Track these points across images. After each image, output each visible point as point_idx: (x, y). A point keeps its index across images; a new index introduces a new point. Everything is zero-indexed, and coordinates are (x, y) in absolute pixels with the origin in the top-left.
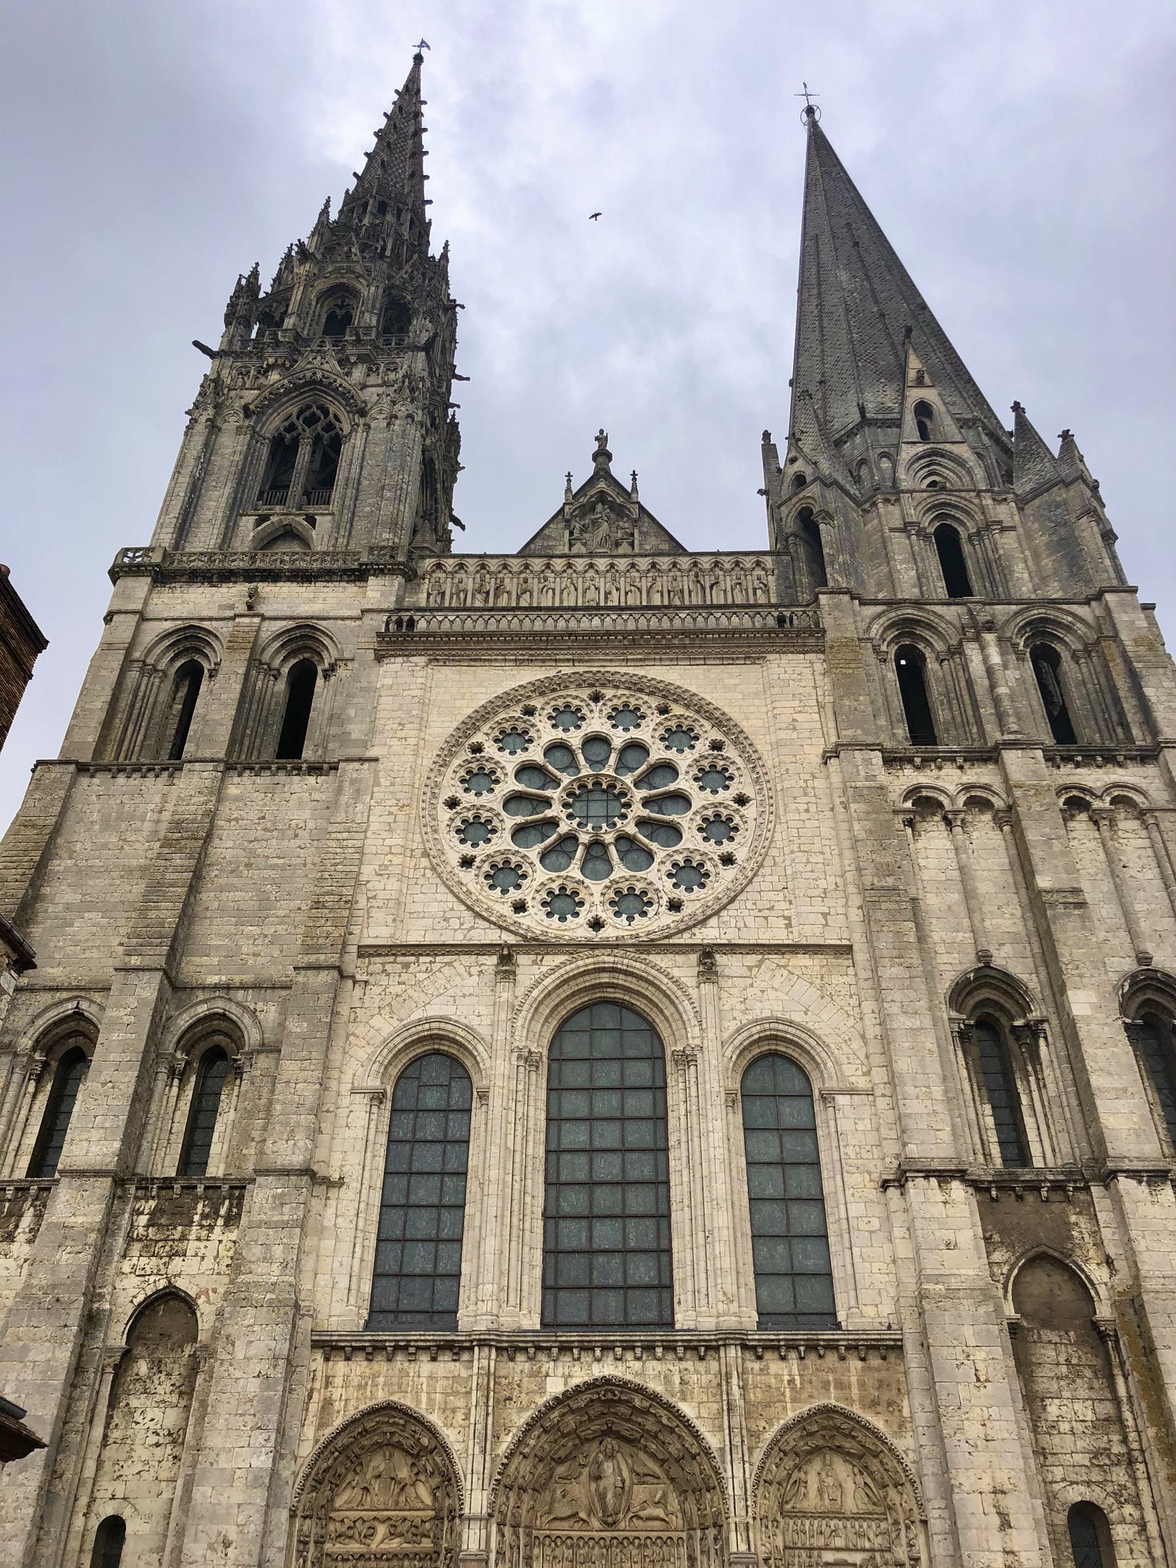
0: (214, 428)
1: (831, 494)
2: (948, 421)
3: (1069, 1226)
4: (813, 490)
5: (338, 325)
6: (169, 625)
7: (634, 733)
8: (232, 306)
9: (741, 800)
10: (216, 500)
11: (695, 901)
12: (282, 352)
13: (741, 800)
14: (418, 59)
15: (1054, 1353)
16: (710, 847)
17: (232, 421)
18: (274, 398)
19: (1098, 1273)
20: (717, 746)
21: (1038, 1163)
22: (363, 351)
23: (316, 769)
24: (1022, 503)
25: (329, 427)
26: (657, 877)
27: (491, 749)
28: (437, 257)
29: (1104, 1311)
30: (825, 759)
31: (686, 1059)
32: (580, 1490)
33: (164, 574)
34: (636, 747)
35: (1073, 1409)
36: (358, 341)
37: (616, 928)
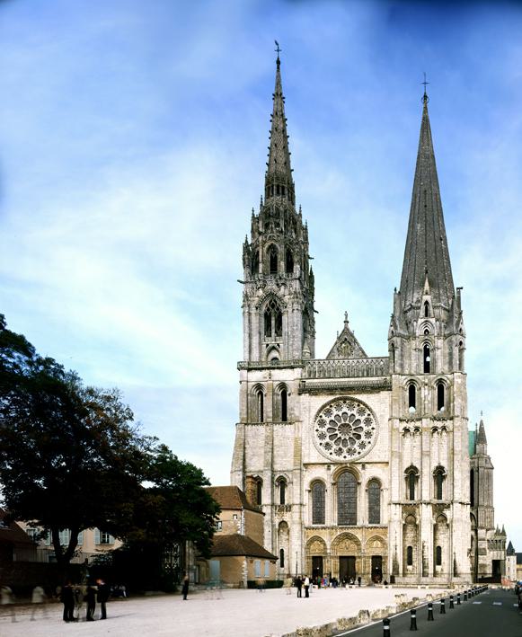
0: (250, 314)
1: (399, 340)
2: (431, 309)
3: (415, 510)
4: (394, 339)
5: (274, 268)
6: (254, 383)
7: (353, 412)
8: (244, 260)
9: (373, 429)
10: (255, 340)
11: (363, 452)
12: (261, 283)
13: (373, 429)
14: (278, 62)
15: (410, 528)
16: (367, 440)
17: (253, 311)
18: (263, 301)
19: (418, 517)
20: (369, 415)
21: (416, 498)
22: (283, 282)
23: (290, 424)
24: (445, 337)
25: (278, 309)
26: (356, 446)
27: (324, 416)
28: (298, 213)
29: (417, 522)
30: (390, 420)
31: (359, 484)
32: (344, 545)
33: (249, 370)
34: (353, 415)
35: (410, 535)
36: (280, 278)
37: (349, 458)
